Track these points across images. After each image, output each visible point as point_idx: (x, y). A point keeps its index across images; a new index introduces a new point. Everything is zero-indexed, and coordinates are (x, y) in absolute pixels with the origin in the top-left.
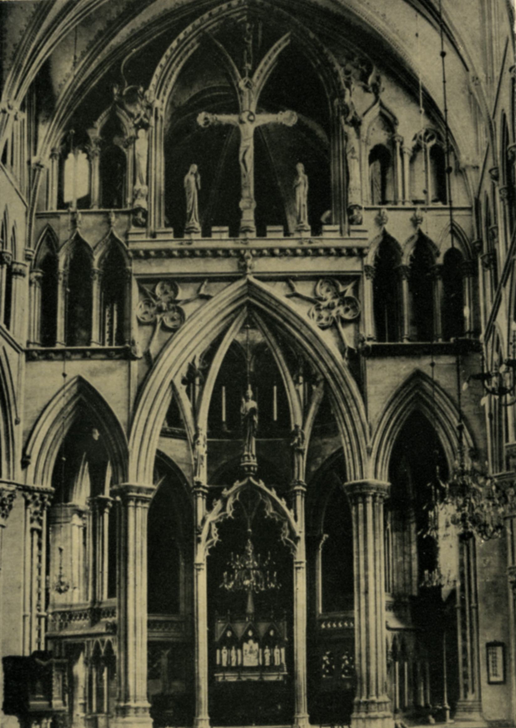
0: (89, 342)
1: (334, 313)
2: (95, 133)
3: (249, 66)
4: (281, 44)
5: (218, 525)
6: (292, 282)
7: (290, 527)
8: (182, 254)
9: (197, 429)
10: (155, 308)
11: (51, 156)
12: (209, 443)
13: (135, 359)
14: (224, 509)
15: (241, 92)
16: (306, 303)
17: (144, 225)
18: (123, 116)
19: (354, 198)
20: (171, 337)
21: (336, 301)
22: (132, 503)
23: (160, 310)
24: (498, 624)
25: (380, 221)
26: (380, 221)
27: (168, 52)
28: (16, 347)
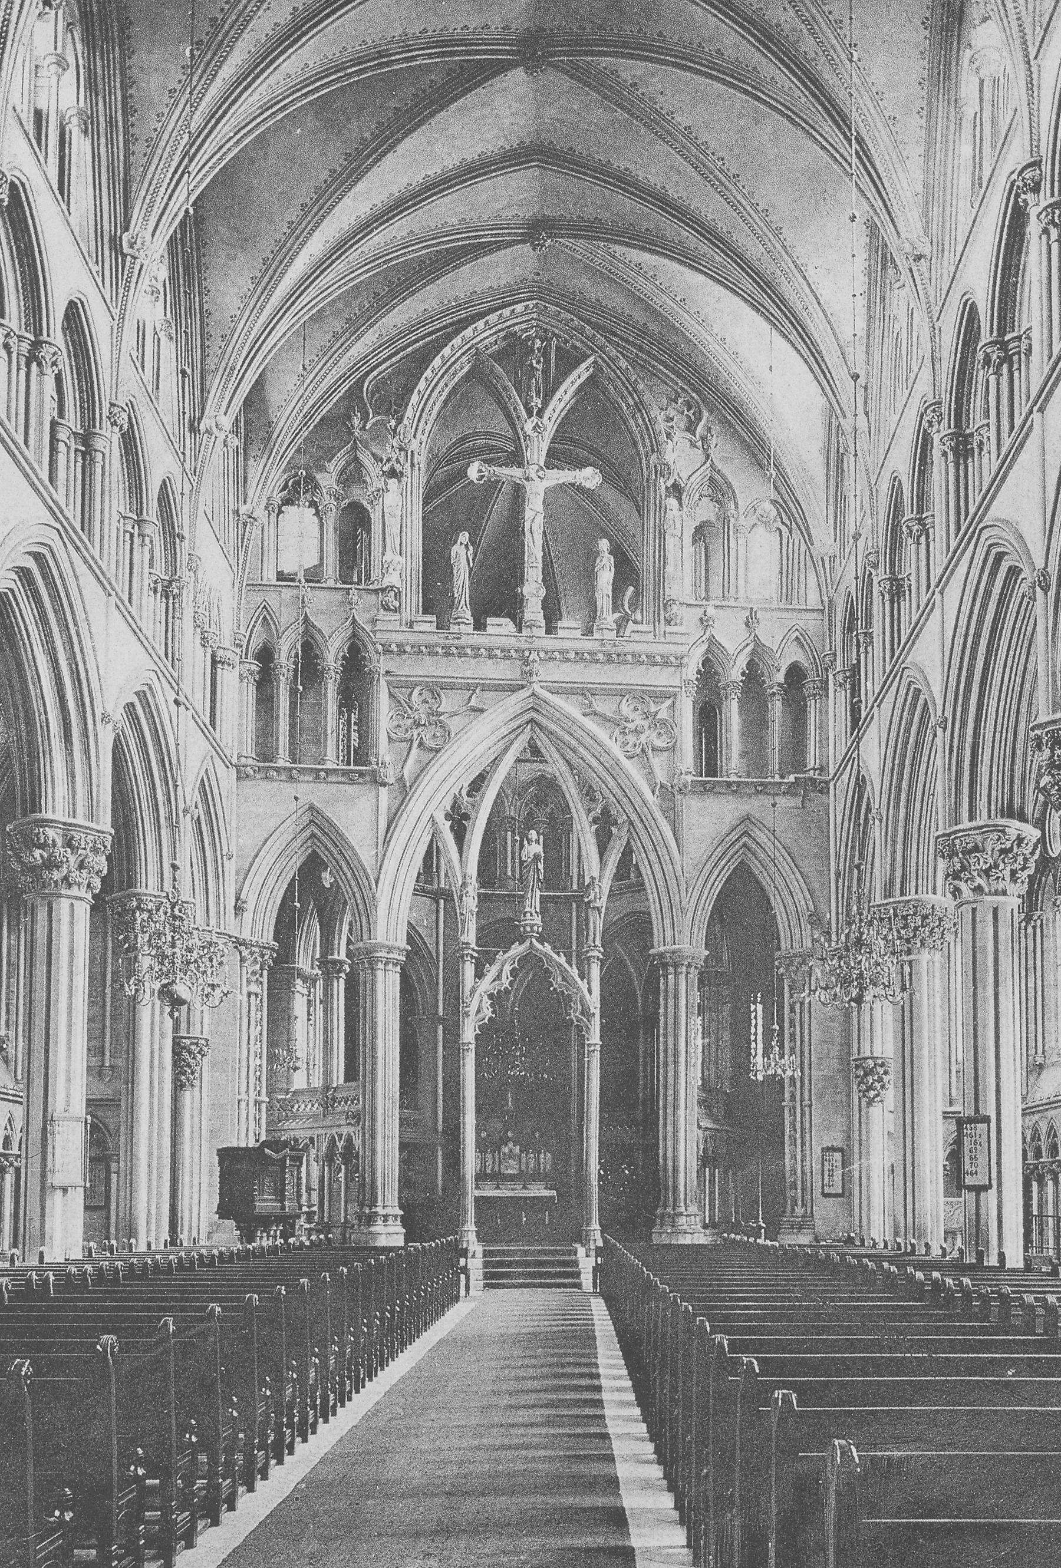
0: (323, 761)
3: (537, 402)
4: (582, 373)
5: (491, 996)
10: (411, 720)
11: (266, 508)
12: (479, 895)
13: (384, 785)
14: (498, 977)
15: (526, 437)
19: (672, 591)
20: (433, 758)
22: (380, 966)
27: (428, 373)
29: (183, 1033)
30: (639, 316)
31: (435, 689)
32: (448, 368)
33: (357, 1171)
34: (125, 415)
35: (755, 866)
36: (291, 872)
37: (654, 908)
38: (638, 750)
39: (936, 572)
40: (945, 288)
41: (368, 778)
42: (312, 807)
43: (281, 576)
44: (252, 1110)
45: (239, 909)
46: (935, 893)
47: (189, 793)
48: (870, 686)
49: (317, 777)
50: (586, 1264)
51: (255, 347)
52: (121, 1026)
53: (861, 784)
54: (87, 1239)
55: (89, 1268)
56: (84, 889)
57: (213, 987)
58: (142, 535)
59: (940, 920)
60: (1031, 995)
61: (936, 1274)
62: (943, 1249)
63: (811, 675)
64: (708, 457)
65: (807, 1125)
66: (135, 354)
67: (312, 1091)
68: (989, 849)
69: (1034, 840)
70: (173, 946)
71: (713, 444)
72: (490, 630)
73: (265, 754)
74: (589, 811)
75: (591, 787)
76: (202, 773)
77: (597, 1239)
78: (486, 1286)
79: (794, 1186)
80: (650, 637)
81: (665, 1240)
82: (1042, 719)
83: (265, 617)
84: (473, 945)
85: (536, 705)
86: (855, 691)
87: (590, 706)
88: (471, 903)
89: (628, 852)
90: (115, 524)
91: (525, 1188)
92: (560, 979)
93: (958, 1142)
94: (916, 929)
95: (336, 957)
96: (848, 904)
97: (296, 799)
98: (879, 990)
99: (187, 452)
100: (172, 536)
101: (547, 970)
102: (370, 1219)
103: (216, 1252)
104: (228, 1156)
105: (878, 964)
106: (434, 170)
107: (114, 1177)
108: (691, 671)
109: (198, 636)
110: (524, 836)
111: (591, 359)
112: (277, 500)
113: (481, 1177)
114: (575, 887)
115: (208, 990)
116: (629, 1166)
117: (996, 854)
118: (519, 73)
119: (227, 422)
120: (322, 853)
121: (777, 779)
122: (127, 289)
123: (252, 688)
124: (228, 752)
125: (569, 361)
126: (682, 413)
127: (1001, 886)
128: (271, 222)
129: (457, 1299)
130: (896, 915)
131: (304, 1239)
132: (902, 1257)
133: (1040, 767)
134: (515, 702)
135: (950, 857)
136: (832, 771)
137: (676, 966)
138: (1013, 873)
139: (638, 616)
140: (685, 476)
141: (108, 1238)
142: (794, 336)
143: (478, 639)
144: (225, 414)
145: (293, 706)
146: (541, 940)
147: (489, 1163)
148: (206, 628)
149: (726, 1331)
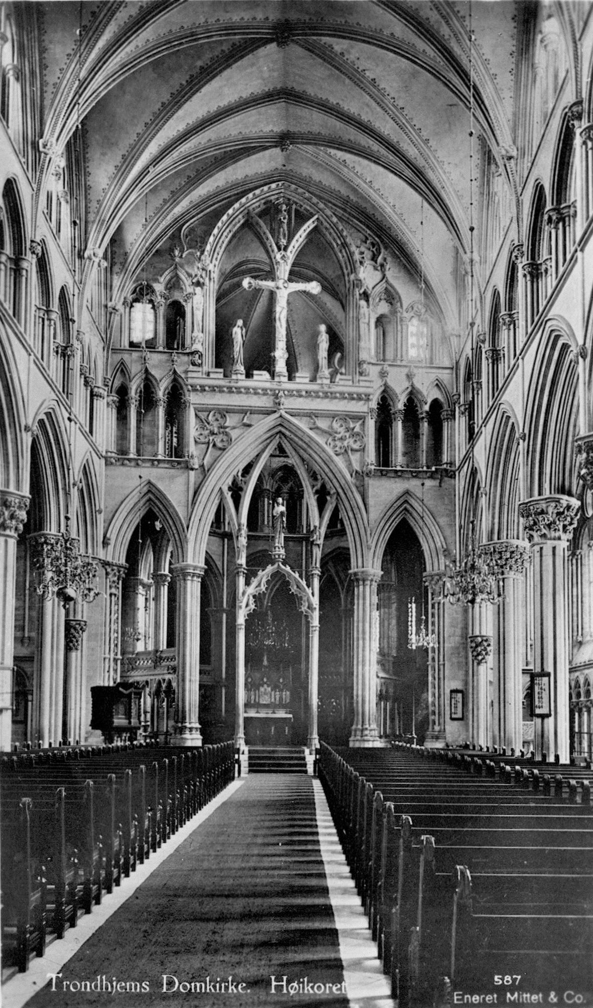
0: (156, 455)
2: (159, 287)
3: (283, 242)
4: (309, 225)
5: (254, 596)
7: (308, 600)
8: (230, 390)
9: (239, 525)
11: (123, 304)
12: (248, 536)
13: (192, 469)
14: (259, 585)
15: (278, 263)
17: (200, 365)
18: (183, 276)
23: (212, 433)
24: (461, 674)
27: (220, 224)
28: (100, 456)
29: (71, 618)
30: (344, 191)
31: (223, 412)
32: (232, 219)
33: (174, 701)
34: (39, 248)
35: (412, 523)
36: (137, 521)
37: (351, 546)
38: (343, 451)
39: (520, 346)
40: (525, 176)
41: (183, 465)
42: (149, 483)
43: (132, 344)
44: (112, 664)
45: (105, 543)
46: (518, 538)
47: (76, 473)
49: (153, 464)
50: (310, 759)
51: (118, 207)
52: (34, 614)
53: (474, 472)
54: (13, 740)
55: (15, 758)
56: (13, 531)
57: (90, 590)
58: (49, 320)
59: (521, 554)
60: (575, 600)
61: (518, 768)
62: (522, 753)
63: (446, 407)
64: (384, 276)
65: (442, 676)
66: (46, 211)
67: (146, 653)
68: (550, 513)
69: (577, 507)
70: (66, 565)
71: (388, 267)
72: (255, 377)
73: (123, 451)
74: (313, 486)
75: (315, 472)
76: (85, 461)
77: (316, 744)
78: (250, 771)
79: (434, 713)
80: (350, 383)
81: (357, 745)
82: (583, 433)
84: (244, 566)
85: (282, 423)
86: (471, 417)
87: (314, 423)
88: (243, 541)
89: (336, 512)
90: (33, 313)
91: (274, 713)
92: (295, 587)
93: (531, 689)
94: (507, 559)
95: (162, 572)
96: (467, 545)
97: (140, 477)
98: (485, 596)
99: (77, 270)
100: (67, 320)
101: (288, 582)
102: (182, 730)
103: (90, 749)
104: (98, 693)
105: (484, 580)
106: (224, 103)
107: (30, 703)
108: (374, 404)
109: (83, 380)
110: (275, 501)
111: (316, 217)
112: (130, 298)
113: (247, 705)
114: (305, 532)
115: (86, 592)
116: (336, 699)
117: (555, 515)
118: (274, 45)
119: (100, 252)
120: (156, 510)
121: (425, 469)
122: (42, 172)
123: (114, 411)
124: (100, 449)
125: (301, 218)
126: (369, 249)
127: (557, 534)
128: (127, 133)
129: (233, 779)
130: (495, 551)
131: (142, 742)
132: (498, 756)
133: (581, 464)
134: (271, 420)
135: (528, 517)
136: (457, 465)
137: (364, 581)
138: (565, 526)
139: (343, 370)
140: (370, 287)
141: (26, 740)
142: (436, 205)
143: (249, 383)
145: (139, 421)
146: (284, 564)
147: (253, 697)
148: (87, 375)
149: (394, 800)
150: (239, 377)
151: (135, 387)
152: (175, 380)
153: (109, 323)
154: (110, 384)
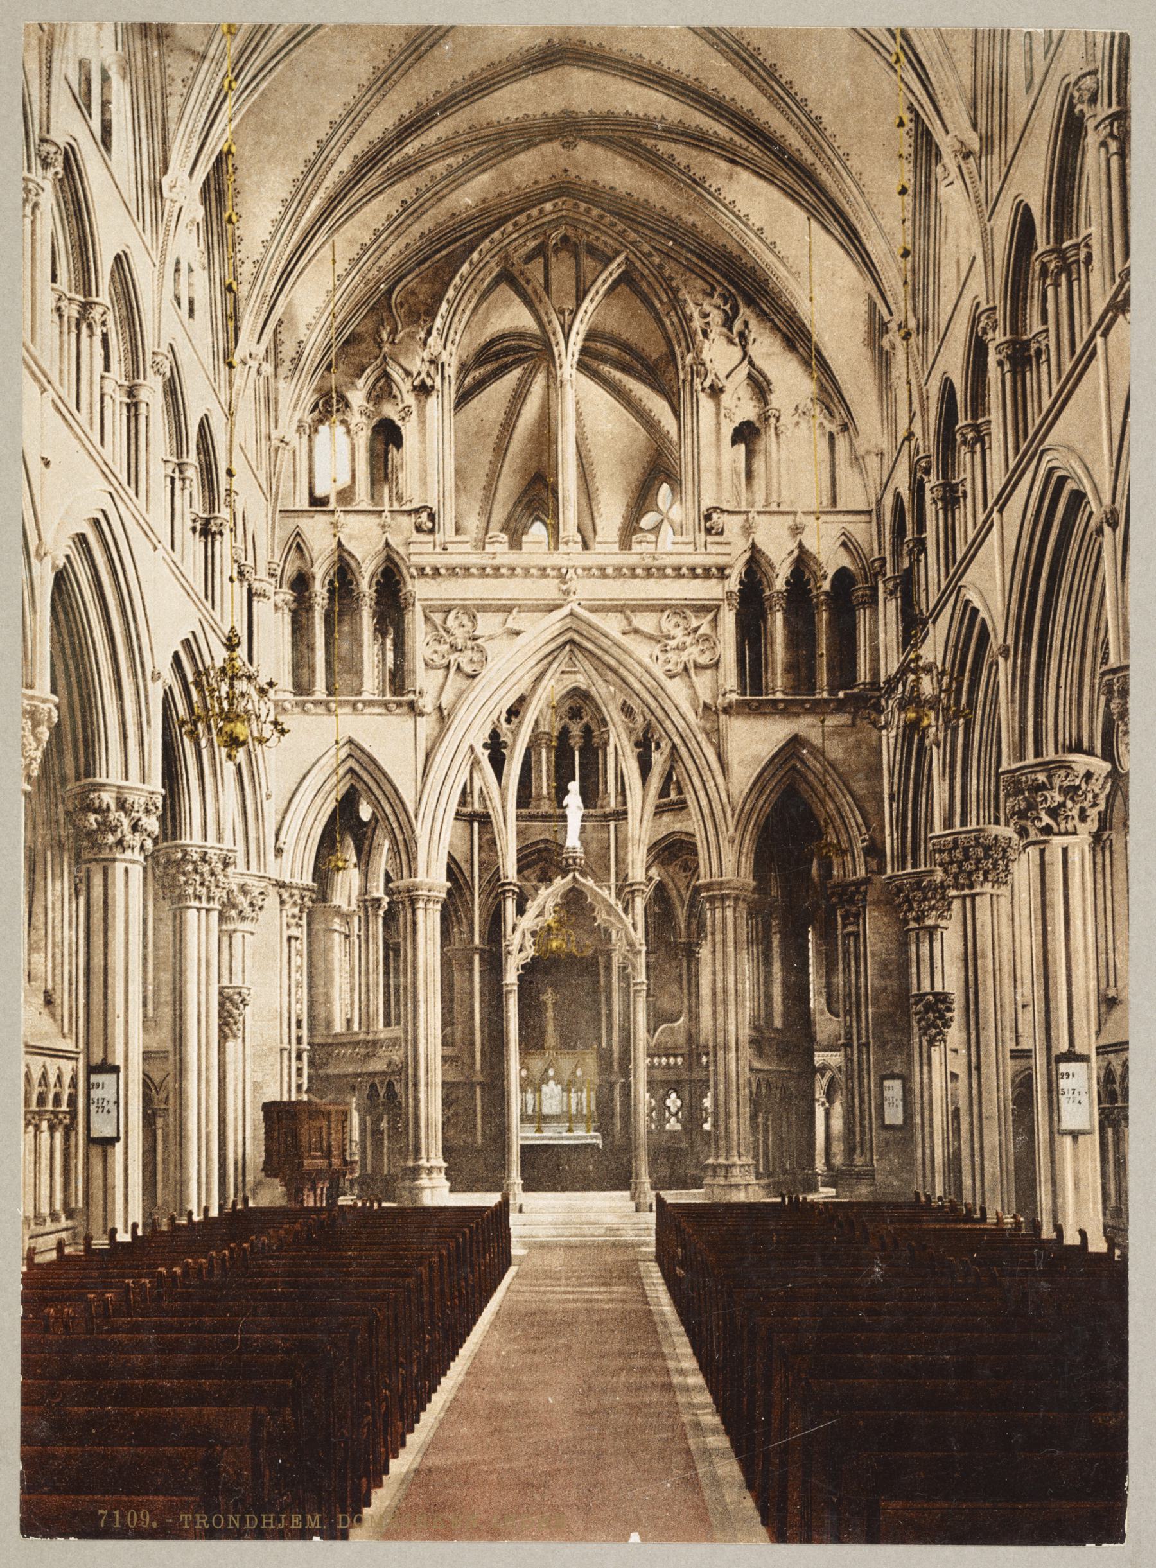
1: (685, 656)
5: (534, 934)
6: (628, 613)
13: (421, 714)
16: (646, 641)
17: (431, 531)
21: (689, 640)
22: (421, 904)
25: (747, 530)
26: (747, 530)
31: (472, 611)
42: (350, 741)
48: (928, 598)
59: (1004, 851)
64: (745, 353)
83: (298, 545)
111: (622, 257)
123: (288, 618)
126: (718, 308)
134: (553, 623)
144: (259, 341)
146: (584, 874)
150: (497, 548)
151: (321, 572)
152: (389, 558)
153: (273, 463)
154: (278, 573)
